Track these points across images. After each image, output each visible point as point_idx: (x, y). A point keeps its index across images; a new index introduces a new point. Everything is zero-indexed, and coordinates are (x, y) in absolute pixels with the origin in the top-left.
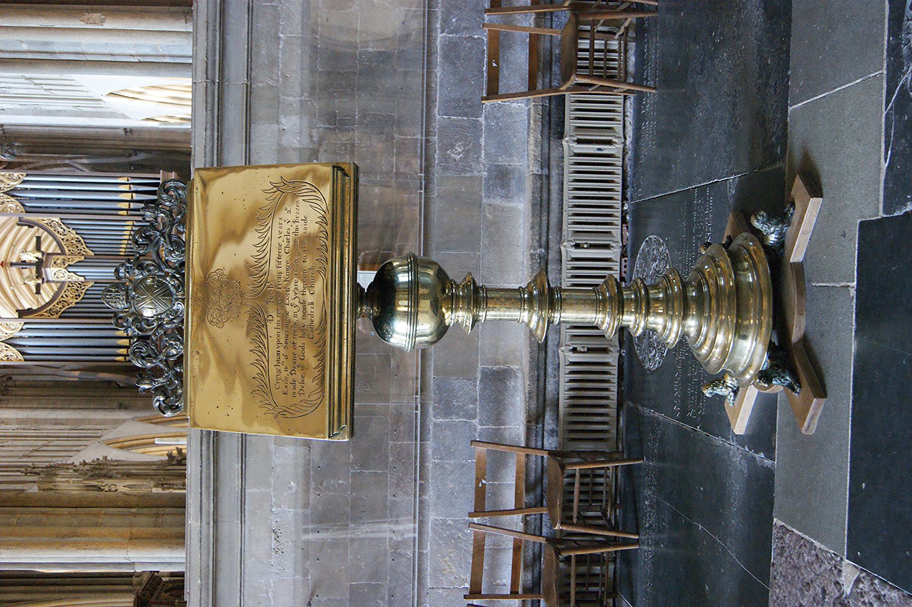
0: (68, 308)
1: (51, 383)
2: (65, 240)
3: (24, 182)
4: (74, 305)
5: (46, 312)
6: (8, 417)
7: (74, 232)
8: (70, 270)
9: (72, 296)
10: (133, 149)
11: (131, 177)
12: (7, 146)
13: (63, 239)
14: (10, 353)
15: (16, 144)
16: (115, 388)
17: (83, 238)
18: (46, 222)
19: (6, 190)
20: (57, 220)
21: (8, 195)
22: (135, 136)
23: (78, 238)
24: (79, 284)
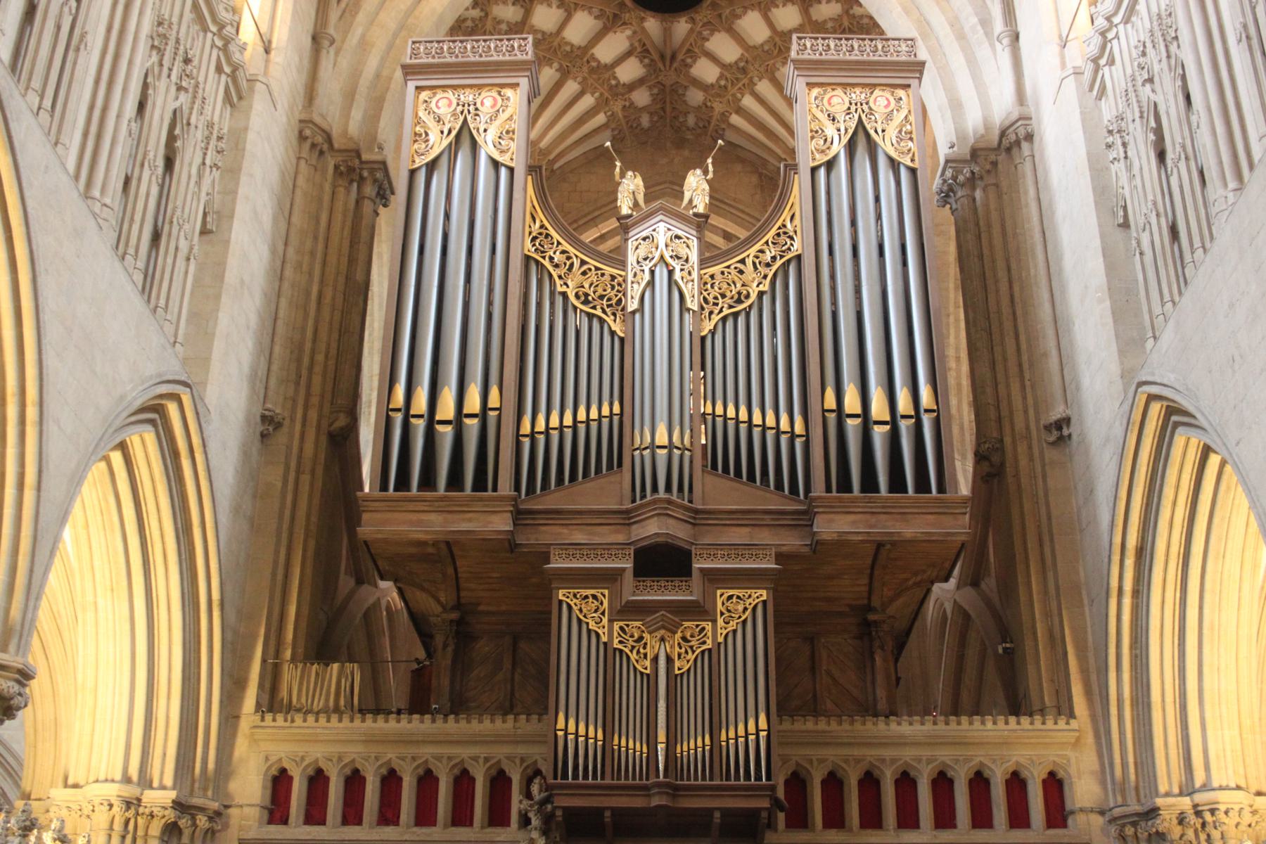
0: (551, 276)
1: (359, 276)
2: (739, 265)
3: (894, 164)
4: (559, 289)
5: (542, 226)
6: (254, 112)
7: (765, 287)
9: (587, 286)
10: (1003, 464)
11: (938, 416)
12: (973, 173)
13: (743, 261)
14: (434, 137)
15: (978, 194)
16: (330, 425)
17: (750, 307)
18: (789, 225)
19: (868, 127)
20: (797, 246)
21: (855, 133)
23: (748, 296)
24: (620, 300)
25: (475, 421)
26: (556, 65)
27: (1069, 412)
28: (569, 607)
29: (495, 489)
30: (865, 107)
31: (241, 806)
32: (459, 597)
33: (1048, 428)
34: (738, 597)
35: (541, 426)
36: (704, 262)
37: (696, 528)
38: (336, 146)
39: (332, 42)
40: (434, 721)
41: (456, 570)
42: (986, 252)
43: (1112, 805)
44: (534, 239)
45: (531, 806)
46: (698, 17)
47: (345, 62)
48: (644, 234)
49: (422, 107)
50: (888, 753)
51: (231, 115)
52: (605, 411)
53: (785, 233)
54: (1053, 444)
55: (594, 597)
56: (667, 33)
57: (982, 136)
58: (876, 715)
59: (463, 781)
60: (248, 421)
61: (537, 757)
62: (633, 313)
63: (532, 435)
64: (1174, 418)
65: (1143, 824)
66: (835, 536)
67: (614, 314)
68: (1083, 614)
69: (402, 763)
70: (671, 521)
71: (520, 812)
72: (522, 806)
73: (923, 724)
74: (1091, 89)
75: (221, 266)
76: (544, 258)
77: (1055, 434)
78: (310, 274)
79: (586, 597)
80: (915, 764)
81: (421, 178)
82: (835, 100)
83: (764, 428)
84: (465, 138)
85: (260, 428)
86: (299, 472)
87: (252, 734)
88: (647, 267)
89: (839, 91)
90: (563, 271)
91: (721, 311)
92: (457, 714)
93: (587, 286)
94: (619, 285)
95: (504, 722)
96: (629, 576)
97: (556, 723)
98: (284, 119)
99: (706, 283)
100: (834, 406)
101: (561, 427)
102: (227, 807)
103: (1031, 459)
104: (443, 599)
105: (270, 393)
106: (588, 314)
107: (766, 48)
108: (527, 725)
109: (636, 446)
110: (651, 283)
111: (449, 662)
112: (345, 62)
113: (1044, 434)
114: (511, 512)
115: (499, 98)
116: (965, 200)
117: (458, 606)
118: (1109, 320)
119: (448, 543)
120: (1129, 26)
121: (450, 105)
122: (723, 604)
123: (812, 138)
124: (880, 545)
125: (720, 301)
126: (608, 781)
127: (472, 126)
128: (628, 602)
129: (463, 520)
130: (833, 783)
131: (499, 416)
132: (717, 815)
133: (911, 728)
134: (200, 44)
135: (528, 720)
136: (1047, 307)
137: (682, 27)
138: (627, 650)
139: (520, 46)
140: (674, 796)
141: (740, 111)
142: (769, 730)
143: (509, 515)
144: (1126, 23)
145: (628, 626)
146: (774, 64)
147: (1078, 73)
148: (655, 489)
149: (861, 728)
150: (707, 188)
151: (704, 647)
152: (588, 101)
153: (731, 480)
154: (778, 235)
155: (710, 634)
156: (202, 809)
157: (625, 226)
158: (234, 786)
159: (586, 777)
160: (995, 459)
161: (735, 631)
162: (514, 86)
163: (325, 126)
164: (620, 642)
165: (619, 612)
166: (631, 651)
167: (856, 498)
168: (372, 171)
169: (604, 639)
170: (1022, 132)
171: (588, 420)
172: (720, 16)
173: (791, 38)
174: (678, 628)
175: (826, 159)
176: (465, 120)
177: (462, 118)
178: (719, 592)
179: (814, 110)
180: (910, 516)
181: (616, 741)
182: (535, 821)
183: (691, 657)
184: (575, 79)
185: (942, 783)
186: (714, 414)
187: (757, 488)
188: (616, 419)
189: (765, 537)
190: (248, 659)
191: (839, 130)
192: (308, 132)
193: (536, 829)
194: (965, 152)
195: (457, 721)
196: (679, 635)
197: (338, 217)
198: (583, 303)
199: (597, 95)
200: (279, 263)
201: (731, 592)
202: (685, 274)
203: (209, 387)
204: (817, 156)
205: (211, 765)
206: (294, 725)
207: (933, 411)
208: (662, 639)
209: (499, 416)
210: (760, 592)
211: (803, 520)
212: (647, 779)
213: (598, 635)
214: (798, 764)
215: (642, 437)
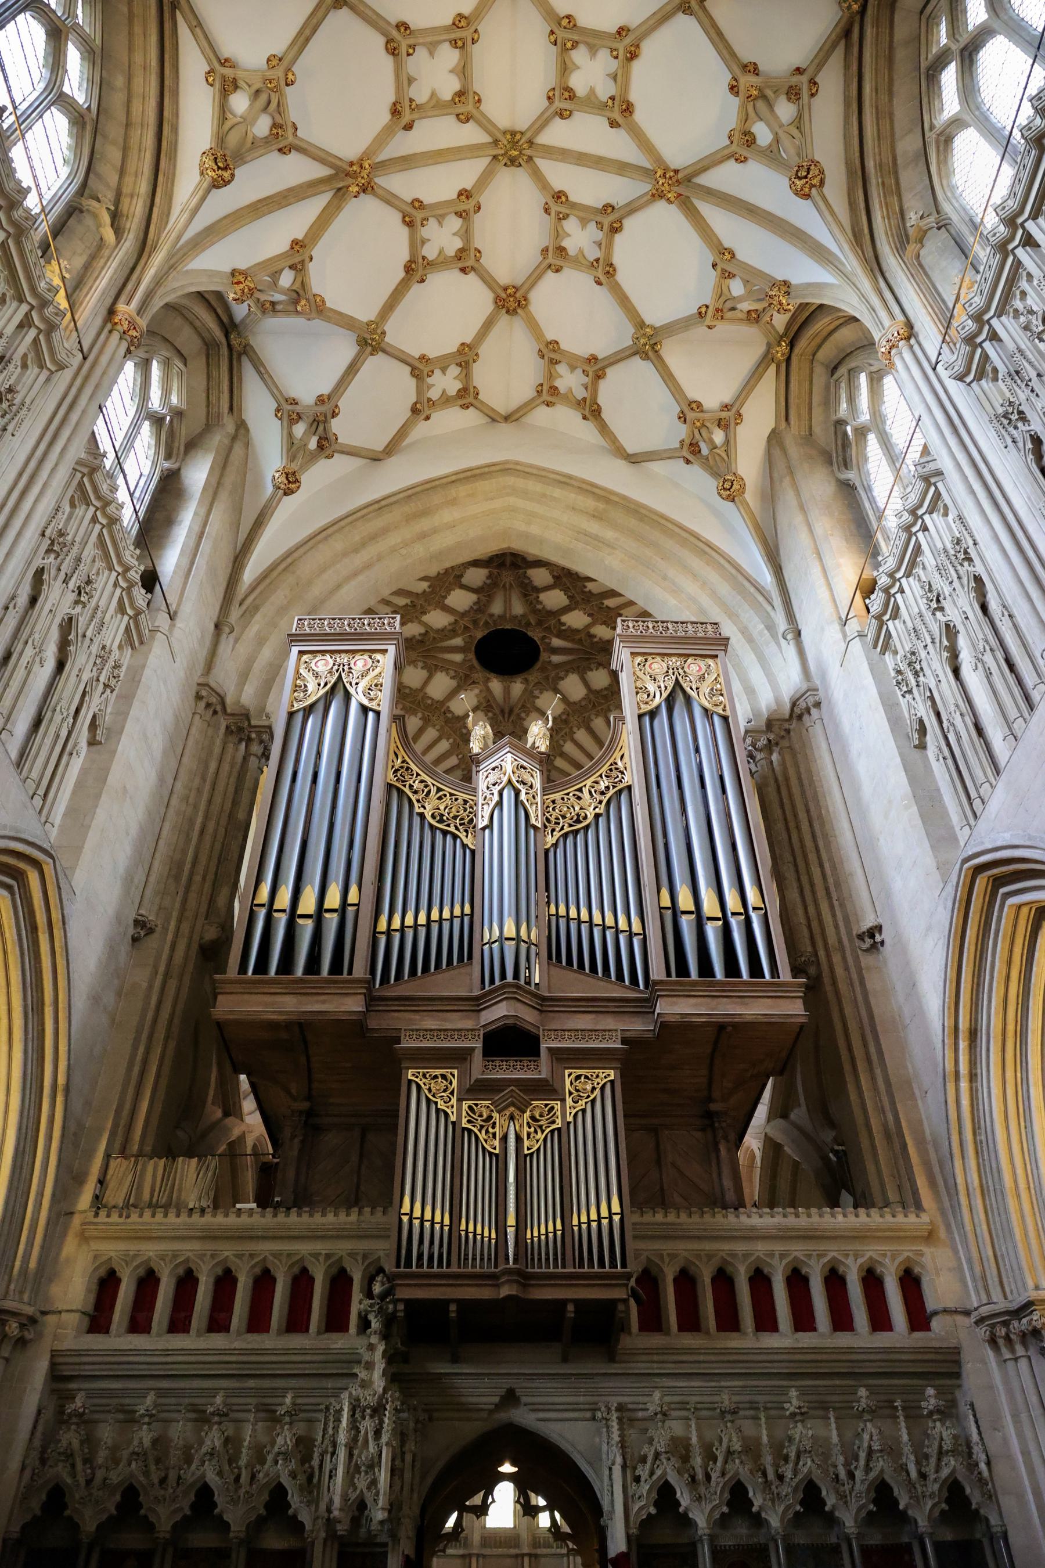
0: (410, 800)
1: (241, 816)
2: (579, 794)
4: (417, 810)
5: (403, 762)
6: (152, 653)
7: (601, 809)
8: (505, 793)
9: (442, 807)
10: (819, 978)
11: (766, 913)
12: (769, 741)
15: (775, 757)
19: (684, 685)
20: (627, 779)
22: (866, 960)
23: (585, 818)
24: (471, 820)
25: (335, 915)
26: (420, 715)
27: (880, 921)
28: (419, 1087)
29: (350, 973)
30: (681, 671)
31: (60, 1312)
32: (310, 1089)
33: (861, 937)
34: (586, 1077)
35: (396, 924)
36: (545, 791)
37: (543, 1015)
38: (229, 711)
39: (232, 631)
40: (275, 1215)
41: (308, 1061)
42: (786, 801)
43: (976, 1305)
44: (396, 771)
45: (372, 1306)
46: (530, 678)
47: (243, 649)
48: (493, 765)
49: (303, 666)
50: (740, 1247)
51: (132, 656)
52: (457, 912)
53: (616, 769)
54: (867, 950)
55: (444, 1077)
56: (507, 691)
57: (775, 711)
58: (725, 1207)
59: (302, 1281)
60: (119, 919)
61: (381, 1254)
62: (484, 829)
63: (389, 933)
64: (1002, 890)
65: (1015, 1323)
66: (678, 1018)
67: (466, 831)
68: (916, 1106)
69: (237, 1261)
70: (519, 1005)
71: (360, 1314)
72: (362, 1306)
73: (772, 1217)
74: (875, 647)
75: (105, 771)
76: (405, 786)
77: (869, 941)
78: (196, 807)
79: (436, 1077)
80: (768, 1260)
81: (299, 718)
82: (654, 666)
83: (604, 928)
84: (338, 691)
85: (131, 931)
86: (167, 975)
87: (83, 1231)
88: (496, 790)
89: (658, 659)
90: (421, 796)
91: (562, 829)
92: (300, 1208)
93: (442, 807)
94: (471, 807)
95: (348, 1215)
96: (478, 1056)
97: (401, 1207)
98: (182, 674)
99: (548, 807)
100: (669, 905)
101: (416, 926)
102: (44, 1313)
103: (847, 969)
104: (293, 1091)
105: (146, 901)
106: (445, 833)
107: (583, 703)
108: (372, 1218)
109: (485, 941)
110: (500, 804)
111: (296, 1153)
112: (243, 649)
113: (857, 942)
114: (365, 994)
115: (370, 661)
116: (763, 762)
117: (309, 1098)
118: (919, 822)
119: (300, 1025)
120: (911, 579)
121: (326, 664)
122: (571, 1083)
123: (637, 693)
124: (721, 1027)
125: (561, 821)
126: (454, 1269)
127: (345, 681)
128: (477, 1080)
129: (317, 1002)
130: (686, 1280)
131: (358, 911)
132: (570, 1307)
133: (761, 1220)
134: (104, 579)
135: (372, 1213)
136: (848, 834)
137: (517, 687)
138: (475, 1130)
139: (389, 623)
140: (525, 1286)
141: (563, 755)
142: (622, 1213)
143: (362, 997)
144: (908, 577)
145: (476, 1105)
146: (589, 717)
147: (861, 635)
148: (503, 976)
149: (712, 1220)
150: (548, 733)
151: (554, 1126)
152: (444, 746)
153: (575, 971)
154: (611, 770)
155: (559, 1113)
156: (14, 1314)
157: (475, 761)
158: (56, 1290)
159: (430, 1265)
160: (812, 971)
161: (584, 1111)
162: (384, 652)
163: (222, 693)
164: (469, 1121)
165: (469, 1091)
166: (480, 1131)
167: (694, 983)
168: (259, 733)
169: (453, 1118)
170: (811, 701)
171: (441, 919)
172: (547, 678)
173: (616, 622)
174: (527, 1107)
175: (649, 708)
176: (340, 676)
177: (337, 675)
178: (567, 1072)
179: (639, 673)
180: (746, 1000)
181: (463, 1227)
182: (375, 1324)
183: (540, 1136)
184: (434, 726)
185: (797, 1281)
186: (557, 915)
187: (599, 979)
188: (466, 919)
189: (609, 1023)
190: (90, 1154)
191: (659, 687)
192: (204, 693)
193: (375, 1333)
194: (762, 724)
195: (299, 1215)
196: (528, 1113)
197: (226, 767)
198: (438, 822)
199: (451, 740)
200: (166, 794)
201: (579, 1072)
202: (530, 796)
203: (78, 871)
204: (642, 706)
205: (33, 1264)
206: (129, 1220)
207: (761, 909)
208: (512, 1118)
209: (358, 911)
210: (607, 1071)
211: (645, 1006)
212: (496, 1267)
213: (446, 1115)
214: (648, 1259)
215: (490, 933)
